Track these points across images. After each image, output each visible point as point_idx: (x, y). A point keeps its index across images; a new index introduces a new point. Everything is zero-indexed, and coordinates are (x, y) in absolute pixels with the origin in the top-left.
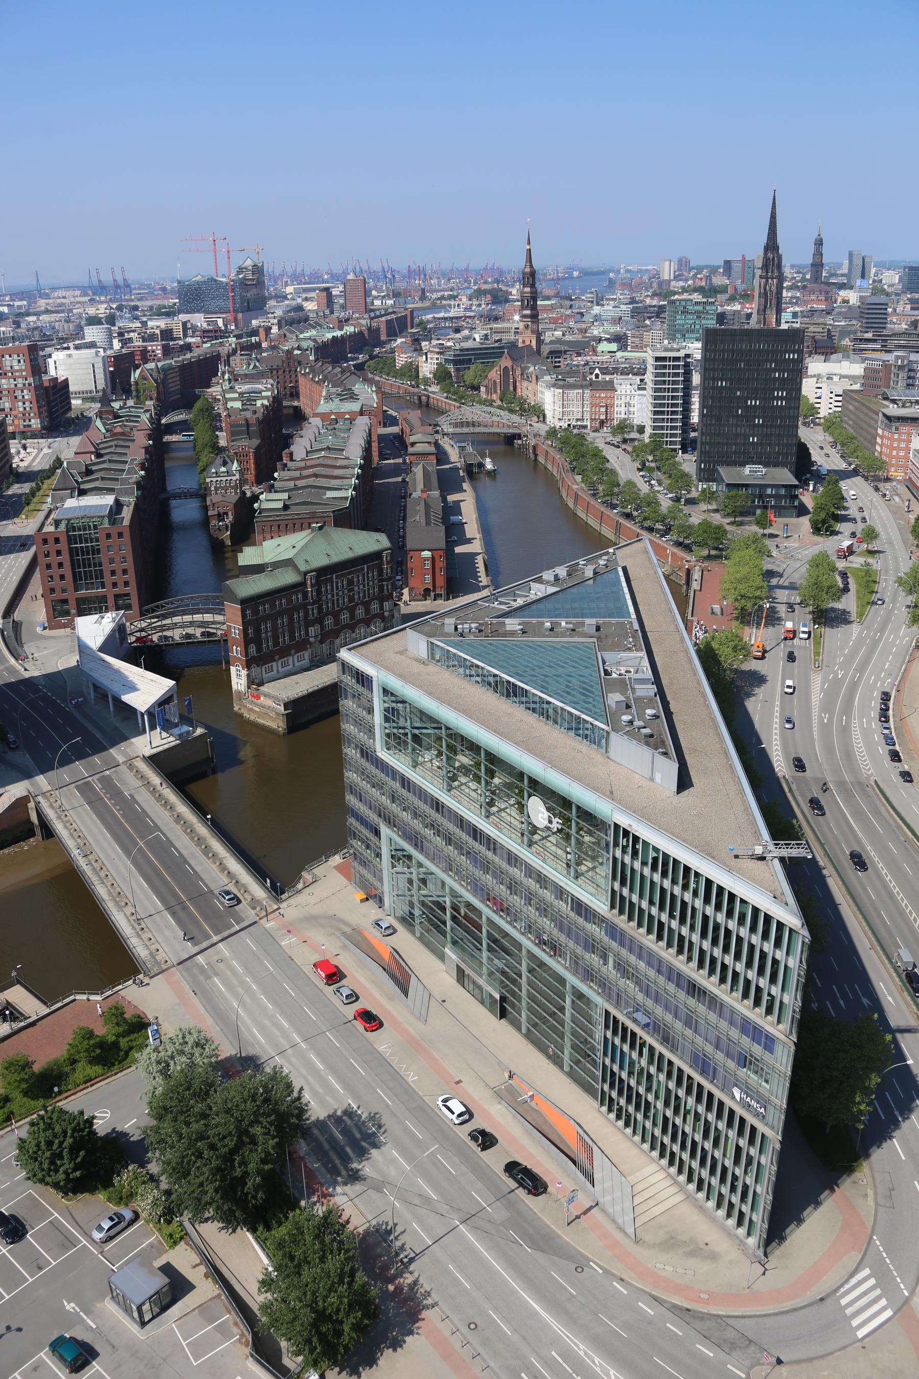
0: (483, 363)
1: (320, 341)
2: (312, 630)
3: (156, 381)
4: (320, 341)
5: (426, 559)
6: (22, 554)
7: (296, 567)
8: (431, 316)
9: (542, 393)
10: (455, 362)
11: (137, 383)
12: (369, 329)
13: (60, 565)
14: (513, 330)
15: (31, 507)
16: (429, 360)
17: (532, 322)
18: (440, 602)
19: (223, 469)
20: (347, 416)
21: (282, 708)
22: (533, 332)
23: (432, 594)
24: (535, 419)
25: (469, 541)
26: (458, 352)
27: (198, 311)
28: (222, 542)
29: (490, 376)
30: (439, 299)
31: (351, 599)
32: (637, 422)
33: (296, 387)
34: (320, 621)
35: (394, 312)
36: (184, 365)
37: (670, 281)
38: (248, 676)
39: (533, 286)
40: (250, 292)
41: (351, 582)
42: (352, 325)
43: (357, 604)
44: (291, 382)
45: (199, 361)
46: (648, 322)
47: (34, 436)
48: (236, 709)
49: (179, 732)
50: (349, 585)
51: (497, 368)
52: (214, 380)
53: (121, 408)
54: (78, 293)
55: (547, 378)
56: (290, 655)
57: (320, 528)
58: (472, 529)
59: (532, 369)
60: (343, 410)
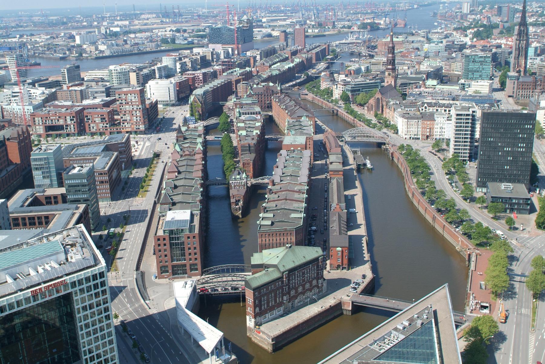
1: (282, 70)
2: (285, 298)
3: (201, 103)
4: (282, 70)
5: (339, 251)
6: (142, 224)
7: (278, 269)
10: (352, 91)
11: (191, 104)
12: (307, 59)
13: (165, 250)
15: (144, 189)
18: (345, 271)
19: (238, 177)
20: (299, 149)
21: (271, 341)
22: (392, 77)
23: (341, 268)
24: (393, 131)
25: (358, 226)
26: (353, 86)
27: (218, 43)
28: (237, 217)
29: (370, 102)
30: (342, 28)
31: (304, 281)
32: (446, 137)
33: (270, 103)
34: (289, 293)
35: (320, 46)
36: (214, 89)
37: (467, 14)
38: (255, 322)
39: (393, 53)
40: (245, 36)
41: (303, 273)
42: (298, 57)
43: (306, 283)
44: (268, 101)
45: (222, 86)
46: (454, 55)
47: (142, 133)
48: (248, 334)
49: (224, 359)
50: (303, 274)
52: (229, 98)
53: (186, 130)
54: (154, 16)
56: (274, 309)
57: (290, 247)
58: (361, 218)
59: (392, 103)
60: (297, 143)
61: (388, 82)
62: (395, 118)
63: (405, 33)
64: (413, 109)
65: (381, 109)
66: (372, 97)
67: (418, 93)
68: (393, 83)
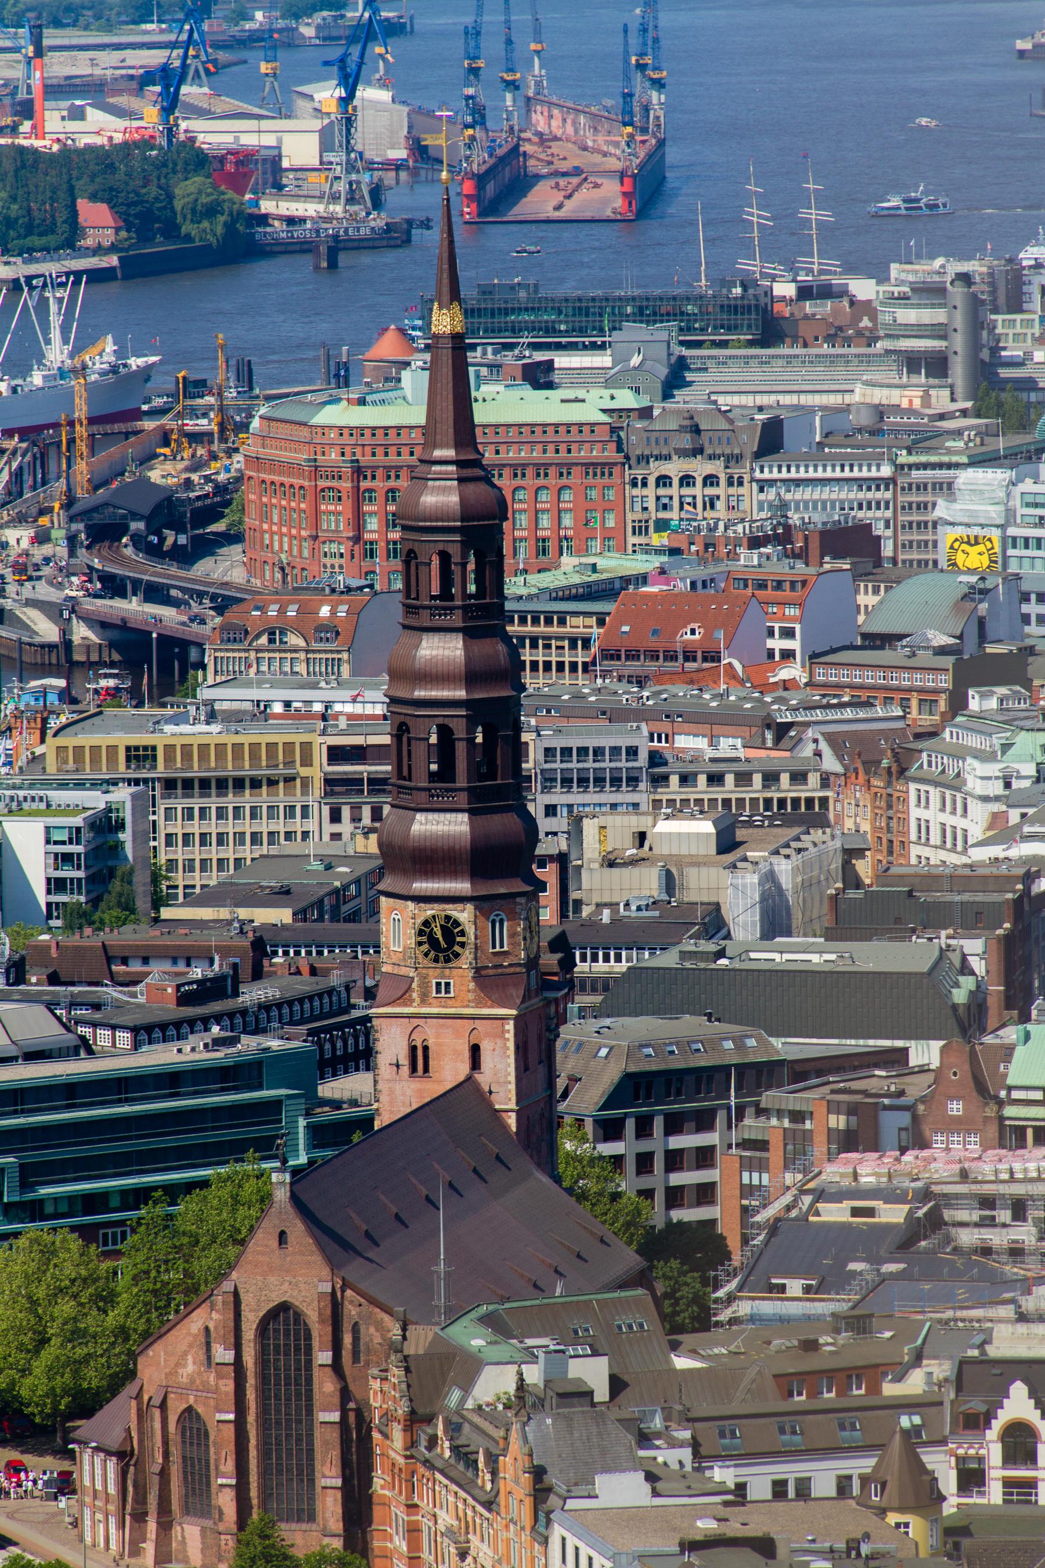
0: (92, 1202)
14: (320, 768)
17: (482, 903)
22: (489, 980)
39: (485, 617)
59: (495, 1384)
61: (419, 1060)
63: (648, 312)
64: (823, 1475)
65: (329, 1477)
67: (893, 1214)
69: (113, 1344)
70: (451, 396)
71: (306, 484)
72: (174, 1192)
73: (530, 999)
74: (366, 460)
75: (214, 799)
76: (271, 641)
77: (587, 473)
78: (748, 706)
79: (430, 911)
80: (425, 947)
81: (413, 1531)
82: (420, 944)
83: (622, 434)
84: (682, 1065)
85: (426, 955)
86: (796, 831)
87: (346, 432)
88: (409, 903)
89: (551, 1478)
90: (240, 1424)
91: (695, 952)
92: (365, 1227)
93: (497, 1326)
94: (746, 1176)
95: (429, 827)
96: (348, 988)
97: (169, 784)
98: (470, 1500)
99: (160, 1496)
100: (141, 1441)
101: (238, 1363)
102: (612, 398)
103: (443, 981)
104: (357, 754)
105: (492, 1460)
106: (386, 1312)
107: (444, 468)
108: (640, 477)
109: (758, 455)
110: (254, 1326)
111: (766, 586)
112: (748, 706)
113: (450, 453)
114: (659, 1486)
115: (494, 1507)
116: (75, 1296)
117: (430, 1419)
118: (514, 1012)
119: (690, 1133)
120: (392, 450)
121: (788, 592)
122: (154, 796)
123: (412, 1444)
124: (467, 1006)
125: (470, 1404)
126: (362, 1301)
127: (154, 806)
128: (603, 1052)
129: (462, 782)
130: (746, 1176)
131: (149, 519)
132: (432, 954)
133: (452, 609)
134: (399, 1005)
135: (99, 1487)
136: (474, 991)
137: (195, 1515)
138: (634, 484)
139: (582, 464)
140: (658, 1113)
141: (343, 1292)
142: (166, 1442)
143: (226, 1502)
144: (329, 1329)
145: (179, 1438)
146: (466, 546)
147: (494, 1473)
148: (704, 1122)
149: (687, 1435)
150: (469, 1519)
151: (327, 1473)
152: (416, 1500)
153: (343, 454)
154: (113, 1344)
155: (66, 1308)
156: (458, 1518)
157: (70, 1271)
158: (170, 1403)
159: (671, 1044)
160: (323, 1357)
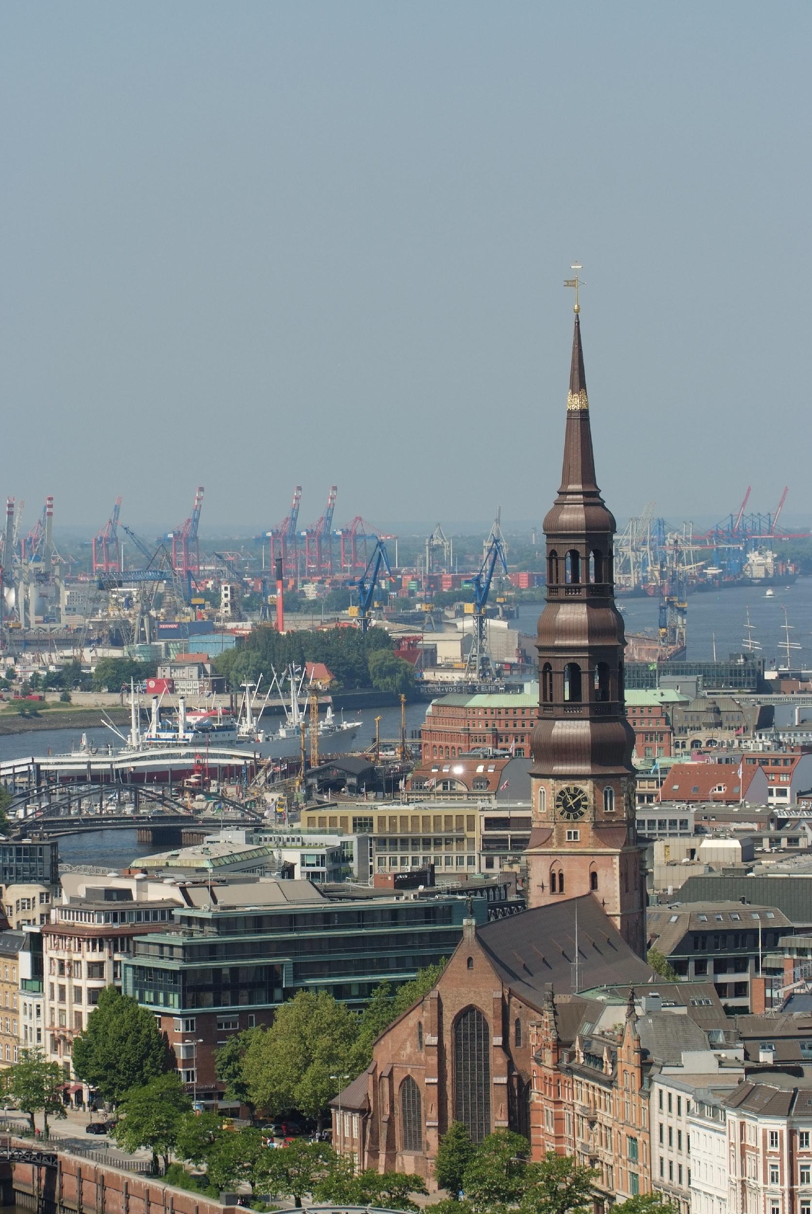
0: (339, 991)
8: (22, 763)
9: (681, 1141)
14: (479, 831)
16: (50, 977)
22: (602, 829)
26: (209, 936)
29: (383, 1056)
39: (601, 595)
51: (423, 1015)
55: (699, 1062)
59: (614, 1016)
61: (557, 882)
62: (659, 1151)
66: (414, 1005)
68: (610, 889)
69: (356, 1065)
70: (580, 450)
71: (462, 745)
72: (394, 985)
73: (629, 845)
74: (501, 728)
75: (410, 852)
76: (445, 788)
77: (646, 739)
78: (758, 810)
79: (564, 785)
80: (561, 809)
81: (558, 1119)
82: (558, 806)
83: (669, 714)
84: (726, 928)
85: (562, 814)
86: (794, 854)
87: (488, 711)
88: (551, 781)
89: (653, 1057)
90: (441, 1085)
91: (733, 869)
92: (523, 962)
93: (613, 993)
94: (768, 992)
95: (564, 730)
96: (505, 887)
97: (382, 842)
98: (597, 1085)
99: (388, 1136)
100: (375, 1102)
101: (440, 1045)
102: (662, 695)
103: (573, 831)
104: (504, 823)
105: (613, 1056)
106: (538, 1012)
107: (575, 497)
108: (680, 741)
109: (758, 727)
110: (451, 1021)
111: (768, 763)
112: (758, 810)
113: (578, 487)
114: (723, 1065)
115: (614, 1084)
116: (331, 1034)
117: (570, 1044)
118: (619, 850)
119: (731, 973)
120: (519, 723)
121: (782, 766)
122: (371, 849)
123: (558, 1061)
124: (589, 847)
125: (596, 1031)
126: (522, 1004)
127: (371, 856)
128: (674, 919)
129: (585, 698)
130: (768, 992)
131: (361, 777)
132: (566, 813)
133: (580, 588)
134: (544, 847)
135: (347, 1135)
136: (593, 837)
137: (411, 1149)
138: (677, 746)
139: (643, 733)
140: (711, 956)
141: (509, 998)
142: (392, 1101)
143: (431, 1137)
144: (501, 1022)
145: (401, 1098)
146: (589, 547)
147: (614, 1063)
148: (740, 966)
149: (741, 1045)
150: (597, 1099)
151: (499, 1118)
152: (560, 1099)
153: (487, 725)
154: (356, 1065)
155: (324, 1041)
156: (589, 1101)
157: (328, 1018)
158: (395, 1074)
159: (719, 914)
160: (497, 1040)
